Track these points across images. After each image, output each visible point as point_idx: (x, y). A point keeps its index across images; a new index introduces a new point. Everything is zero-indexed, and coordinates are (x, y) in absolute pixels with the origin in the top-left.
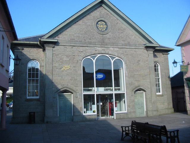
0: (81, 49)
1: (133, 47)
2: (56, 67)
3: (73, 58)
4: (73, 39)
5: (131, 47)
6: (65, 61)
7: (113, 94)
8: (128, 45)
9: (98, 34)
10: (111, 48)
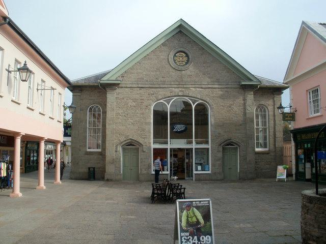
8: (216, 84)
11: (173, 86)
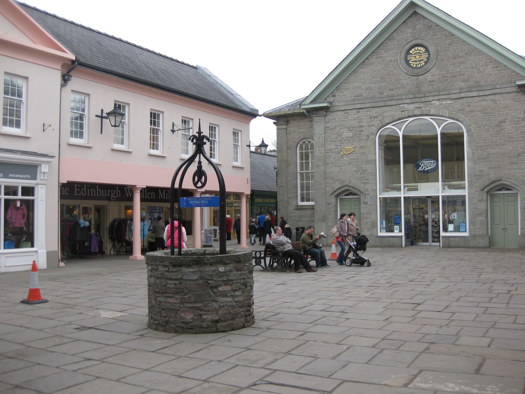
0: (374, 112)
1: (487, 93)
2: (331, 150)
3: (360, 131)
4: (360, 96)
5: (481, 93)
6: (346, 137)
7: (400, 198)
8: (474, 89)
9: (407, 76)
10: (434, 101)
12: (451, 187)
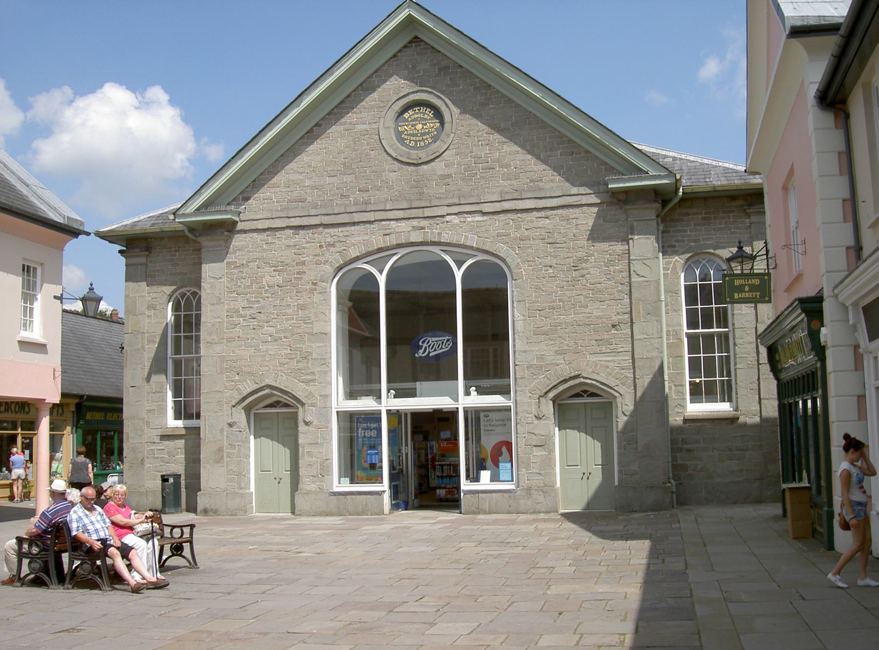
11: (391, 215)
12: (481, 391)
